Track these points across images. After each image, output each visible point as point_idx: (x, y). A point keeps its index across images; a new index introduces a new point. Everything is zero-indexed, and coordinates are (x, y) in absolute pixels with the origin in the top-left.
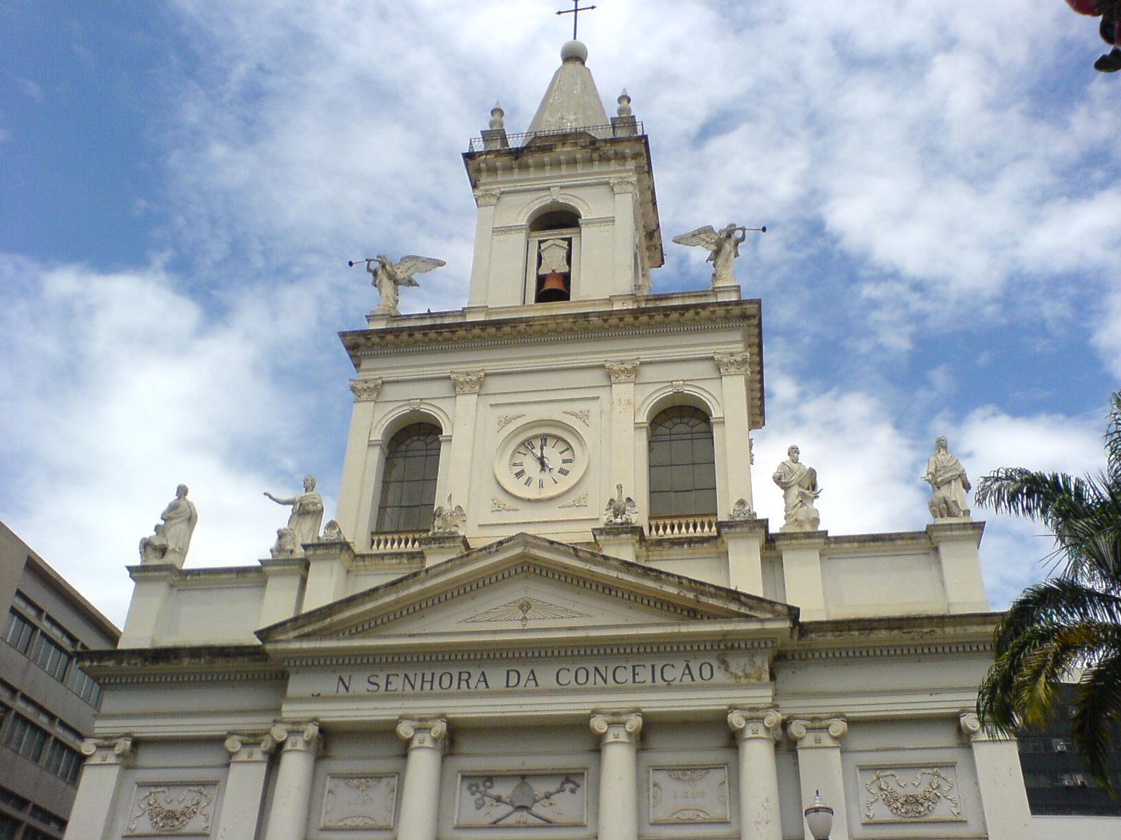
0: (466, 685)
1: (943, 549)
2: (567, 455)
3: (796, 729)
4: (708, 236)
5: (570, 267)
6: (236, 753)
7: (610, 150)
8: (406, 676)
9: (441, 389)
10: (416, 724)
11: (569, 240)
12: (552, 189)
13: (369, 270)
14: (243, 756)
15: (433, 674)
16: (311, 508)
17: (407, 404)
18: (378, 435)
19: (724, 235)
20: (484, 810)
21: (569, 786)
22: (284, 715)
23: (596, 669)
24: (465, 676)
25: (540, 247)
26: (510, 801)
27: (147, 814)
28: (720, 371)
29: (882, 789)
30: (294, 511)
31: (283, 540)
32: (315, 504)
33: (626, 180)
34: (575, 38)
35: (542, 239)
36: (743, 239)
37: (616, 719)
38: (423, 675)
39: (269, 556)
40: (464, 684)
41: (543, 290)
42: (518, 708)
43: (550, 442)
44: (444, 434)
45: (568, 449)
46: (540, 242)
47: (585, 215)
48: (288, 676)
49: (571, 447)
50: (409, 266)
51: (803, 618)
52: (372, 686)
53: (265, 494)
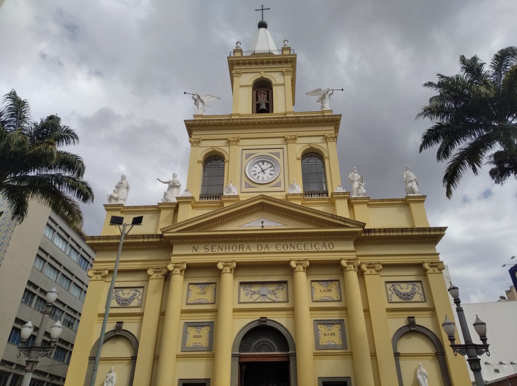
0: (242, 250)
1: (412, 205)
2: (272, 169)
3: (364, 267)
4: (319, 92)
5: (269, 101)
6: (151, 276)
8: (219, 246)
9: (223, 143)
10: (223, 264)
11: (268, 92)
12: (261, 72)
13: (193, 98)
14: (154, 276)
15: (229, 246)
16: (177, 184)
17: (211, 148)
18: (201, 159)
19: (326, 92)
20: (250, 296)
21: (280, 287)
22: (172, 261)
23: (291, 244)
24: (241, 246)
25: (257, 94)
26: (259, 293)
27: (115, 299)
28: (327, 140)
29: (395, 290)
30: (170, 185)
31: (167, 196)
32: (178, 183)
33: (289, 70)
34: (263, 19)
35: (258, 90)
36: (332, 94)
37: (299, 262)
38: (226, 246)
39: (161, 202)
41: (259, 109)
42: (262, 258)
43: (266, 164)
44: (226, 159)
45: (271, 167)
46: (257, 92)
47: (274, 82)
48: (172, 247)
49: (273, 166)
50: (208, 98)
51: (365, 228)
52: (206, 249)
53: (158, 179)
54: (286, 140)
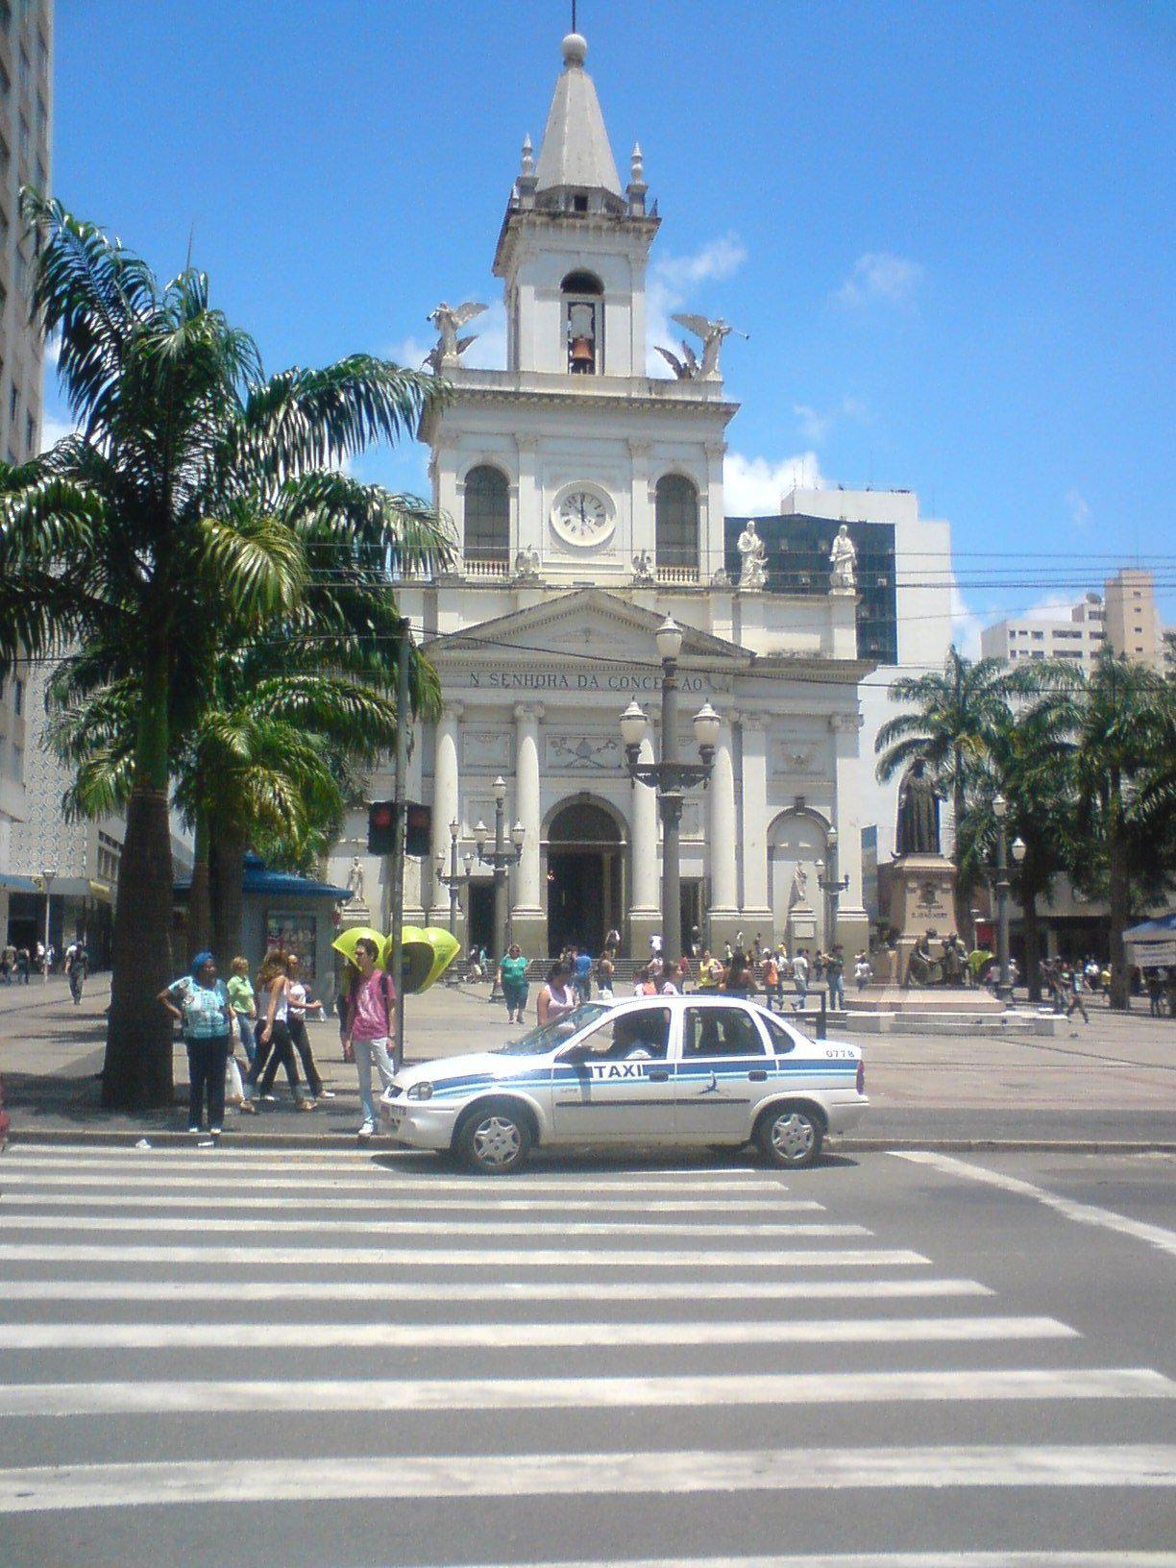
3: (744, 719)
7: (631, 225)
21: (611, 745)
24: (552, 678)
25: (570, 311)
40: (552, 683)
46: (571, 305)
47: (607, 292)
54: (629, 448)
